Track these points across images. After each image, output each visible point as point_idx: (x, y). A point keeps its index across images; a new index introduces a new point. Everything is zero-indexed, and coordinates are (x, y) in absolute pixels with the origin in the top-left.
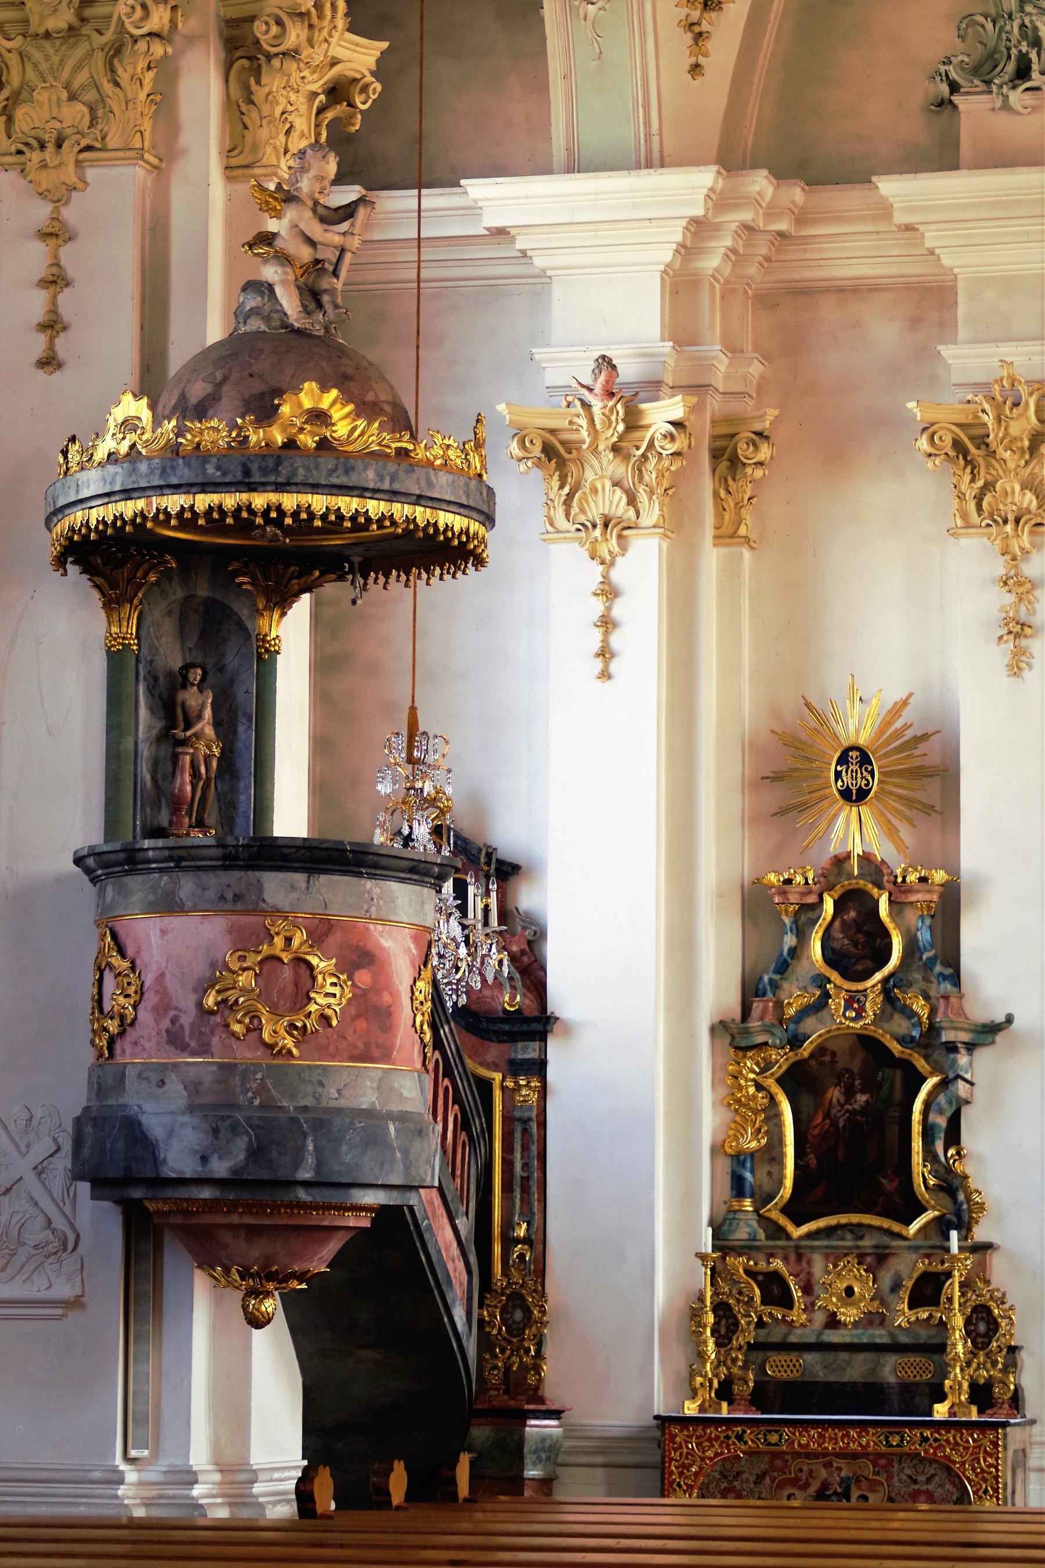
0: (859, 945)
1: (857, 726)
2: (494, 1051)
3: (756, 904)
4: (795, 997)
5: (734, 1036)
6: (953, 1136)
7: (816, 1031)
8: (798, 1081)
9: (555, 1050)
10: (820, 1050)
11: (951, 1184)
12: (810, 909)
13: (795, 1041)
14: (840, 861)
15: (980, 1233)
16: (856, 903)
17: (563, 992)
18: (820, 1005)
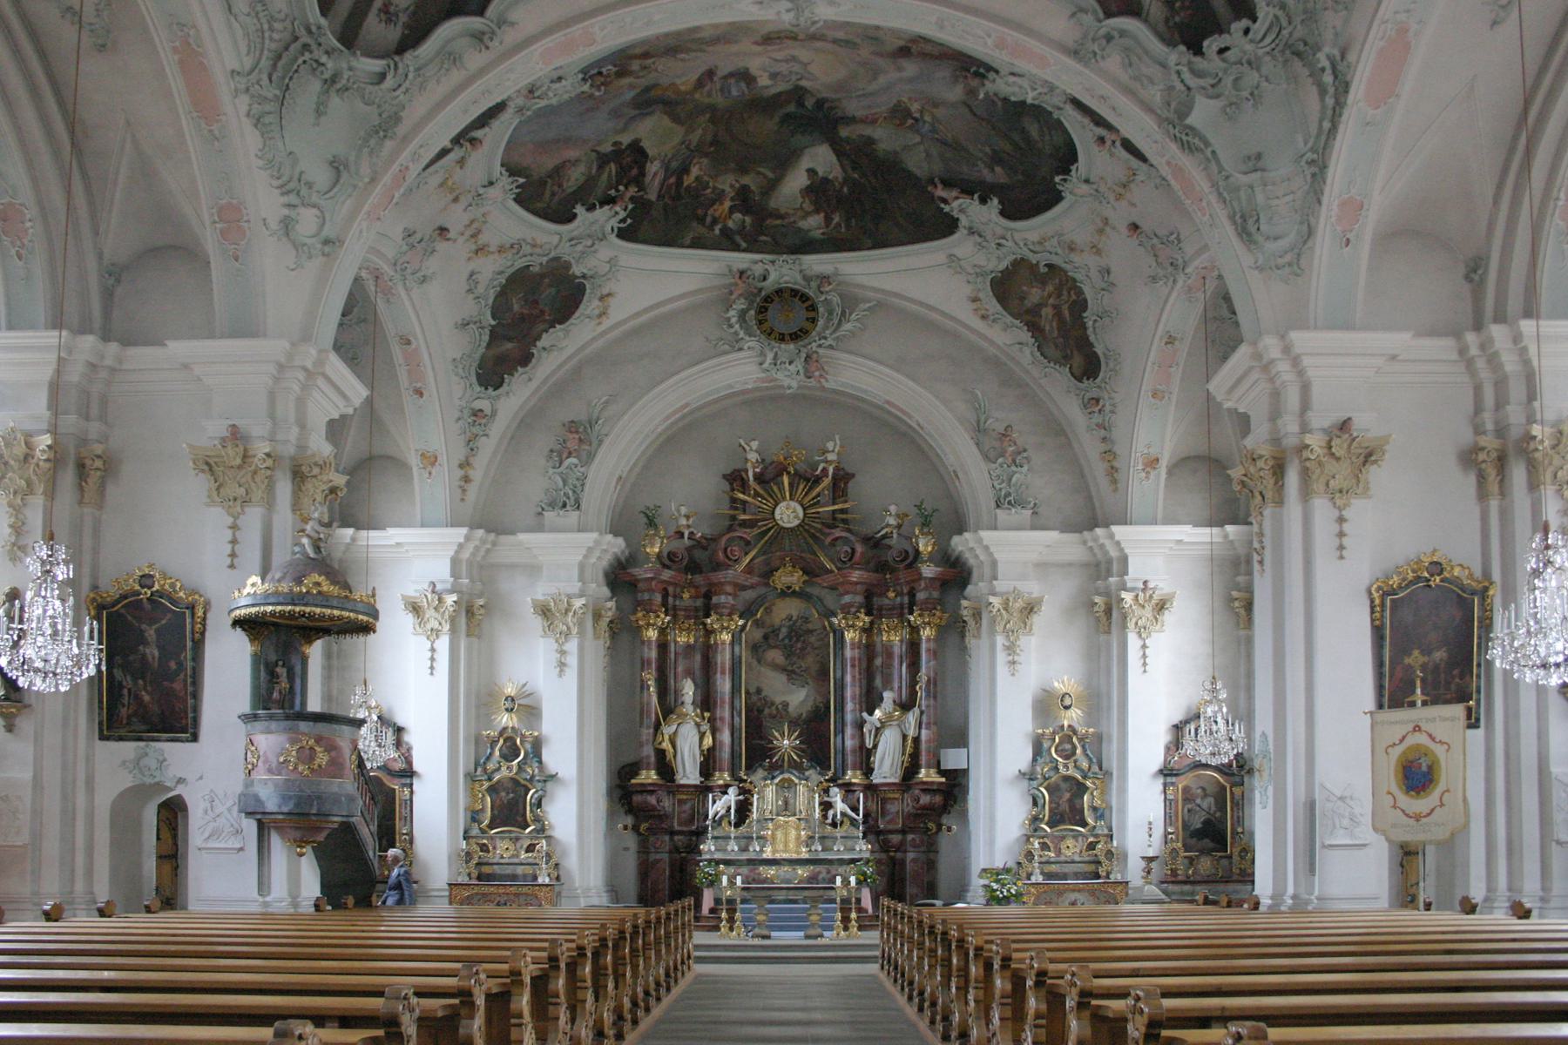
0: (511, 752)
1: (510, 690)
2: (397, 780)
3: (478, 740)
4: (491, 766)
5: (471, 778)
6: (539, 805)
7: (497, 777)
8: (492, 790)
9: (415, 781)
10: (499, 781)
11: (537, 820)
12: (494, 743)
13: (490, 779)
14: (505, 729)
15: (548, 833)
16: (510, 741)
17: (417, 766)
18: (499, 769)
